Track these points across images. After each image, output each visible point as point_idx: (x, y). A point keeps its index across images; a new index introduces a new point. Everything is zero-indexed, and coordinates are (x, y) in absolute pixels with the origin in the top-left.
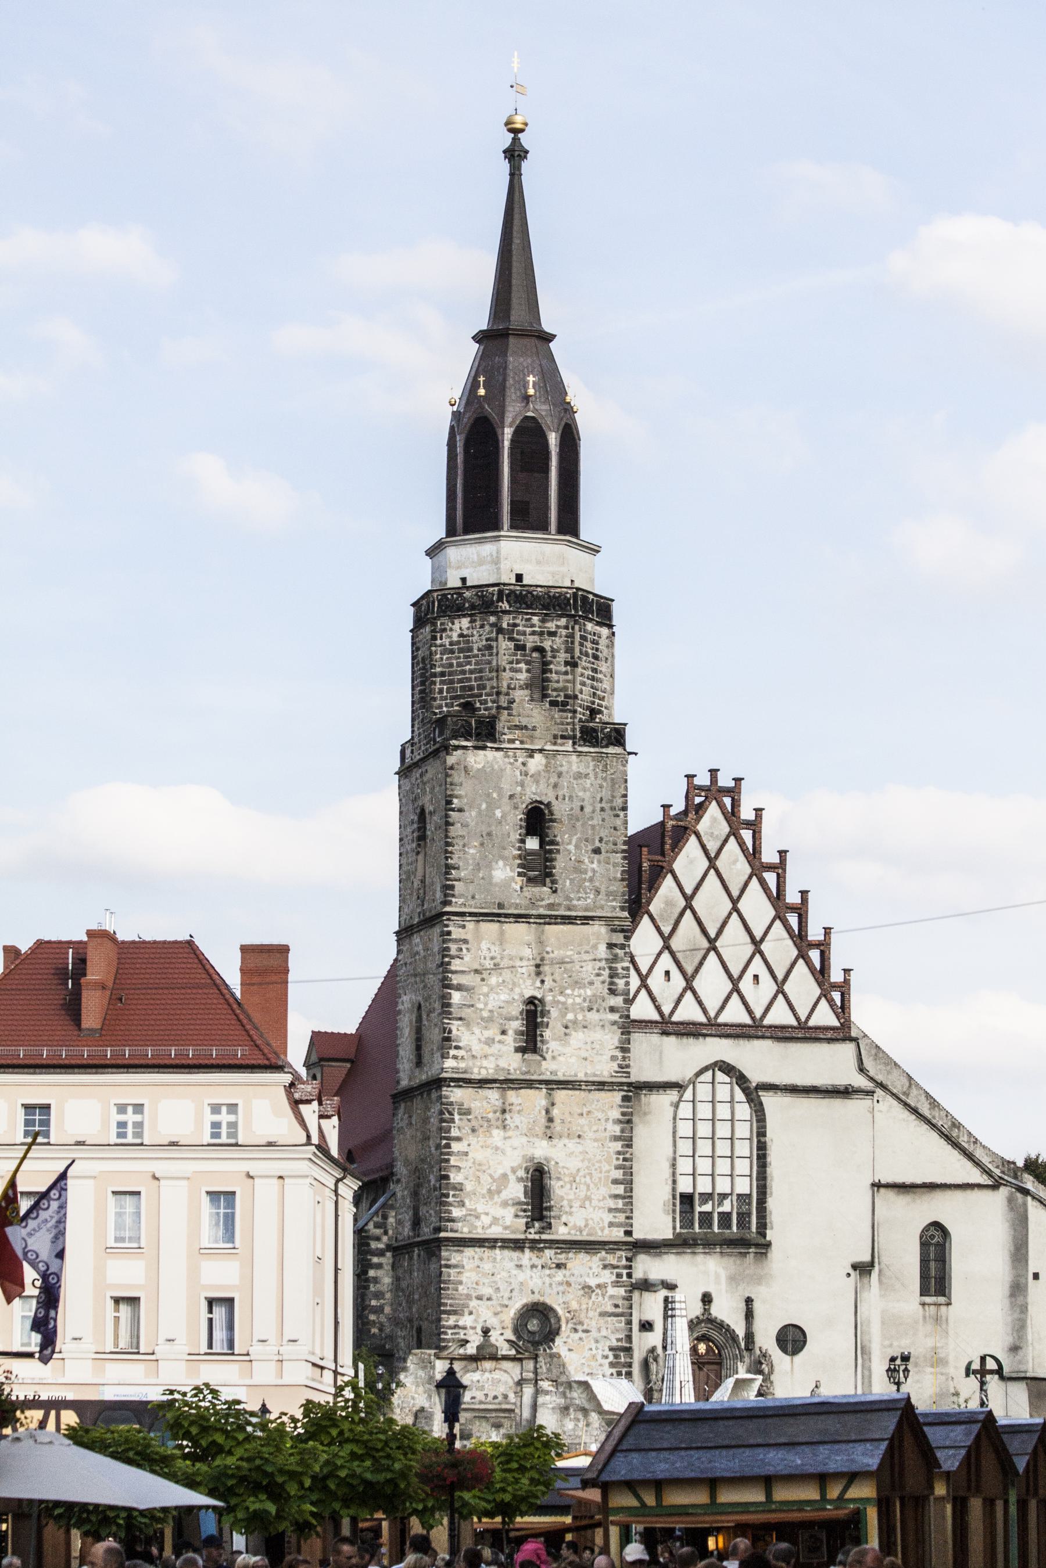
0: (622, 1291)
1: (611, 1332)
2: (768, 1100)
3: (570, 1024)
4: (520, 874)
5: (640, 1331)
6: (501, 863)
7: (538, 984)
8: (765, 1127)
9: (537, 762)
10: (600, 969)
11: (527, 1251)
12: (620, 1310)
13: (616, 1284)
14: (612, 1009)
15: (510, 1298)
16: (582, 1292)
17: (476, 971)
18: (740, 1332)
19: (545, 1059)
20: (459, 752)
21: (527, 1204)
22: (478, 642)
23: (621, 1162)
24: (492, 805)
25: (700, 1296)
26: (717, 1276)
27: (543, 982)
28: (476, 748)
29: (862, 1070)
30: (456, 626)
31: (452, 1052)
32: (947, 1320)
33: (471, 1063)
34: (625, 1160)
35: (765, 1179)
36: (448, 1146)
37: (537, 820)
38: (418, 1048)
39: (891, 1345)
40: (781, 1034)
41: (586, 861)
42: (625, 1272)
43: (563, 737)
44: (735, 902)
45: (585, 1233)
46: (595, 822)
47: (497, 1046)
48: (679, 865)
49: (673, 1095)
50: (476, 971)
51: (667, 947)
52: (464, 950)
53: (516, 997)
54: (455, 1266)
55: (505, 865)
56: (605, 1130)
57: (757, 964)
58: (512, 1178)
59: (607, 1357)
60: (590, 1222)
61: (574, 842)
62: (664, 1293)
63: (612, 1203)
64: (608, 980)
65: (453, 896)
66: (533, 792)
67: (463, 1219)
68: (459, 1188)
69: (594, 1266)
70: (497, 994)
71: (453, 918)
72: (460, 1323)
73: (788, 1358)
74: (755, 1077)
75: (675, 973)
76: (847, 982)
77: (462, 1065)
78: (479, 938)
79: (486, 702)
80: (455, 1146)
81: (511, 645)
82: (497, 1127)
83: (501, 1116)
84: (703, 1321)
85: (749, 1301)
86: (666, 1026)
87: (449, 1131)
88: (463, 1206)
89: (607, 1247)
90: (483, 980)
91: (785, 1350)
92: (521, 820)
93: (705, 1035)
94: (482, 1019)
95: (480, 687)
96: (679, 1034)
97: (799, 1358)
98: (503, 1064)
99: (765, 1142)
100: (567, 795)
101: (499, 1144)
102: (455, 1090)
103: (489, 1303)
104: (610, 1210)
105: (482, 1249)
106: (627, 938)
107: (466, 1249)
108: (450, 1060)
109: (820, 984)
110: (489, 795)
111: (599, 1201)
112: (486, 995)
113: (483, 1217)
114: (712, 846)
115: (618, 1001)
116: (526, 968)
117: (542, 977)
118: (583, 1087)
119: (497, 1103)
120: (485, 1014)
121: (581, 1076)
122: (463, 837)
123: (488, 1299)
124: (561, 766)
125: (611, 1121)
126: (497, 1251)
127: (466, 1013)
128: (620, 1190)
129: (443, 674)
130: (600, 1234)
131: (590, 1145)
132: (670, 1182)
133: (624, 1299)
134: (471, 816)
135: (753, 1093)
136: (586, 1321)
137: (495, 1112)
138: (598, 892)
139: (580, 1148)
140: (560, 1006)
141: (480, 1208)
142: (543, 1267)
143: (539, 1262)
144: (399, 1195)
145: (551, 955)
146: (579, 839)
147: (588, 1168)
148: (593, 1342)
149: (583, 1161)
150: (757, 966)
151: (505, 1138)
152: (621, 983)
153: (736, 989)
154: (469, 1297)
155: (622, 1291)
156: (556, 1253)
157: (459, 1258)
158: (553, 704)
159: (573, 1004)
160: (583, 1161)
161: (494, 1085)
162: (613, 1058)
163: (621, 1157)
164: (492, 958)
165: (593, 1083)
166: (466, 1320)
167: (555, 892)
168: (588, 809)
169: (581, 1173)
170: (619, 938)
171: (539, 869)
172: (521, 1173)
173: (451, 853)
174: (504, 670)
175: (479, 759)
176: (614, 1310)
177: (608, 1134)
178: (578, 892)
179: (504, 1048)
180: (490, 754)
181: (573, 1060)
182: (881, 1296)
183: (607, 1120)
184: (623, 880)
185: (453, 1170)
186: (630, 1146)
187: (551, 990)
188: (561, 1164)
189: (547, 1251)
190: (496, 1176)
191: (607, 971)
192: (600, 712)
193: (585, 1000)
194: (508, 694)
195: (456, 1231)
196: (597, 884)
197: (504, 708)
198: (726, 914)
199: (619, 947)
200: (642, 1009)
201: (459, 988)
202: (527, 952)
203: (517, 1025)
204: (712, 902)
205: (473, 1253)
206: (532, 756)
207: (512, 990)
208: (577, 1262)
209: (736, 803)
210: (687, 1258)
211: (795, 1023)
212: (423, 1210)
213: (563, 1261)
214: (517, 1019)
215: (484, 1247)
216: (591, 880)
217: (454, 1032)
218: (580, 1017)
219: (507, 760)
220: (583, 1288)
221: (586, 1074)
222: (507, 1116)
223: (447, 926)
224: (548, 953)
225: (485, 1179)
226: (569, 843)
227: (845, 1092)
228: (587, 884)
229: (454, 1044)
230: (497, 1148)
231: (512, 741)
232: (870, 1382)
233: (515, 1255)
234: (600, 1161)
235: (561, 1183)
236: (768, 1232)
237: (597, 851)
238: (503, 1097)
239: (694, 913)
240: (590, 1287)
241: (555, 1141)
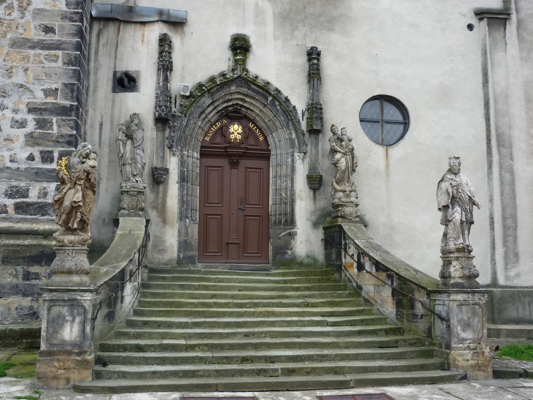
5: (114, 91)
12: (55, 38)
25: (228, 41)
26: (259, 12)
59: (22, 124)
84: (232, 81)
85: (313, 55)
133: (64, 17)
176: (43, 36)
182: (521, 59)
232: (513, 191)
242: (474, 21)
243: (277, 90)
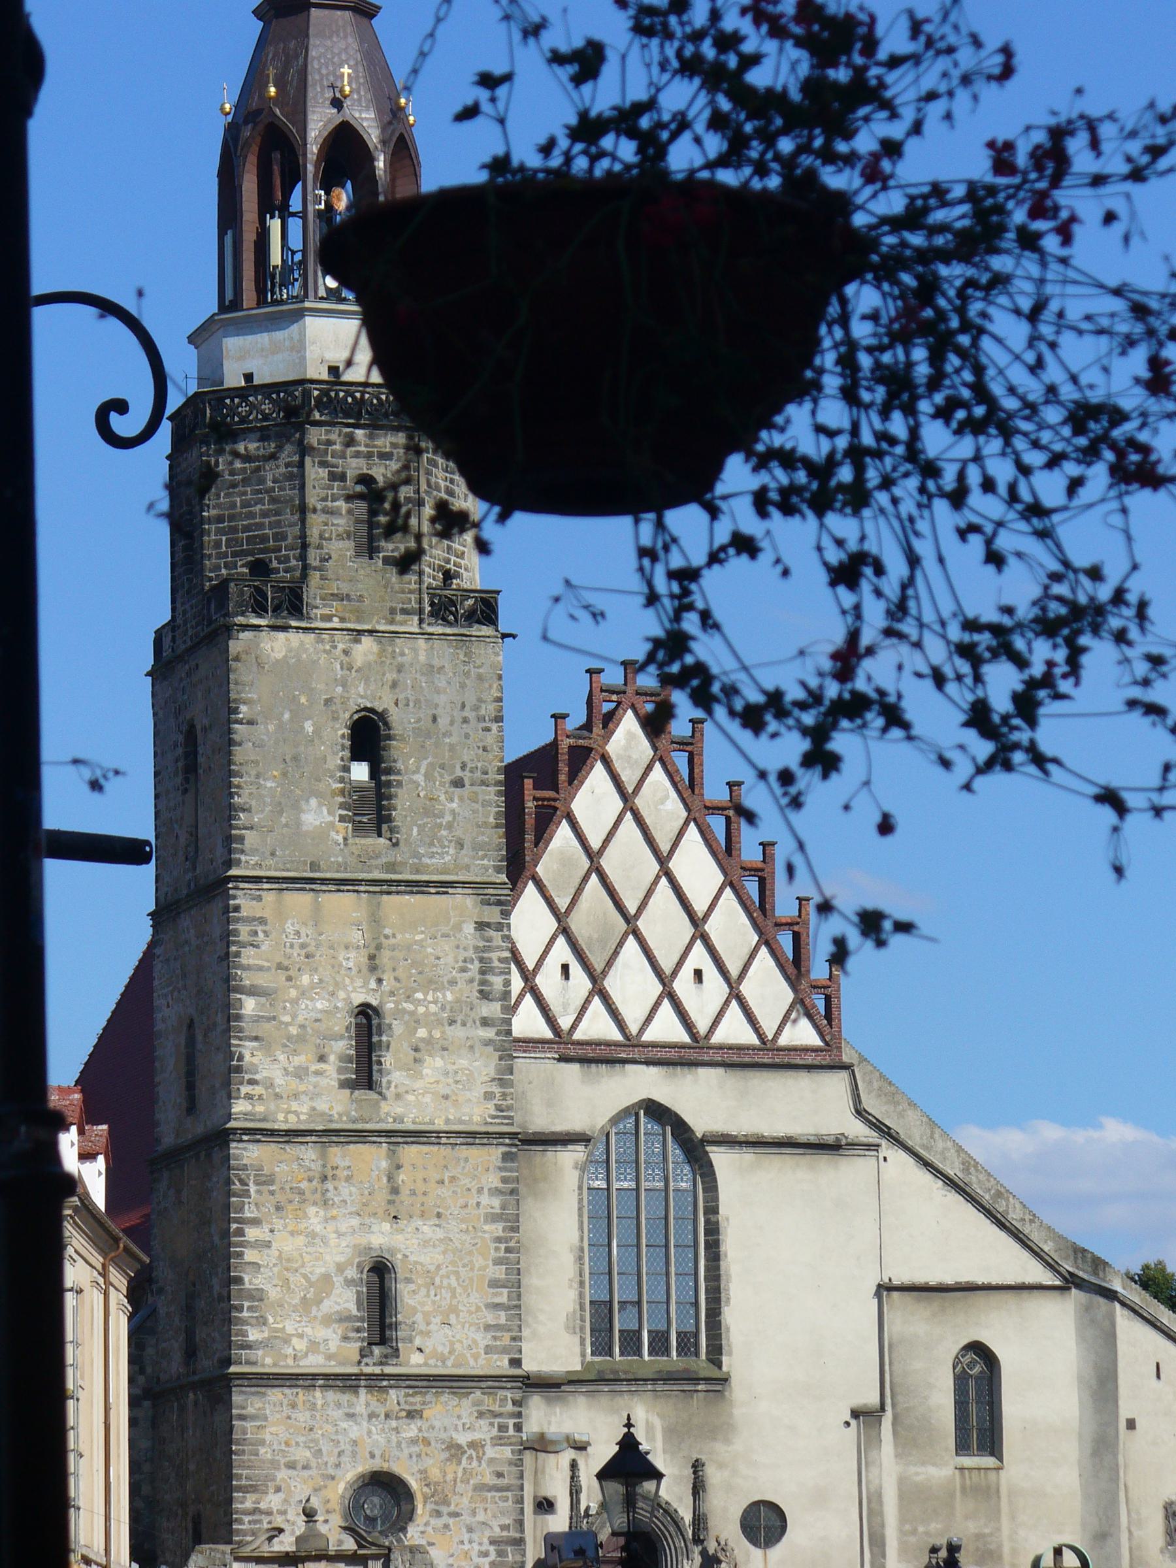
0: (507, 1452)
1: (495, 1517)
2: (720, 1158)
3: (421, 1045)
4: (342, 819)
5: (535, 1513)
6: (313, 802)
7: (373, 984)
8: (716, 1199)
10: (465, 961)
11: (362, 1391)
13: (498, 1441)
14: (485, 1022)
15: (338, 1465)
16: (447, 1455)
17: (280, 967)
18: (686, 1516)
19: (385, 1098)
20: (246, 635)
21: (361, 1320)
23: (502, 1254)
24: (299, 715)
27: (380, 981)
28: (274, 628)
29: (860, 1113)
31: (244, 1090)
32: (998, 1491)
33: (272, 1107)
34: (508, 1250)
35: (717, 1278)
36: (240, 1232)
37: (368, 736)
38: (190, 1087)
39: (914, 1532)
40: (736, 1060)
41: (442, 798)
42: (511, 1422)
43: (405, 612)
44: (663, 861)
45: (449, 1363)
46: (454, 739)
47: (313, 1079)
48: (581, 805)
49: (577, 1153)
50: (280, 967)
52: (261, 935)
53: (339, 1005)
54: (254, 1418)
55: (320, 805)
56: (478, 1204)
58: (338, 1280)
59: (485, 1554)
60: (458, 1346)
61: (423, 771)
62: (569, 1455)
63: (490, 1318)
64: (478, 977)
65: (242, 852)
66: (361, 696)
68: (258, 1296)
69: (465, 1414)
70: (312, 1000)
71: (242, 885)
72: (263, 1506)
73: (757, 1553)
74: (700, 1125)
75: (576, 969)
77: (260, 1109)
79: (287, 559)
80: (252, 1233)
81: (323, 473)
82: (315, 1203)
83: (319, 1186)
85: (697, 1466)
87: (241, 1210)
88: (264, 1324)
89: (483, 1385)
90: (289, 979)
91: (754, 1542)
92: (343, 736)
93: (624, 1062)
94: (289, 1038)
95: (275, 535)
96: (584, 1061)
97: (777, 1552)
98: (322, 1106)
99: (718, 1222)
100: (412, 698)
101: (318, 1229)
102: (250, 1146)
103: (306, 1473)
105: (295, 1390)
106: (506, 914)
107: (269, 1391)
108: (241, 1101)
109: (793, 983)
110: (295, 699)
111: (471, 1313)
112: (295, 1002)
113: (295, 1341)
114: (629, 778)
115: (493, 1009)
116: (354, 959)
117: (379, 974)
118: (444, 1140)
119: (313, 1166)
120: (294, 1030)
121: (440, 1125)
122: (256, 762)
123: (305, 1467)
124: (403, 654)
125: (486, 1190)
126: (318, 1393)
127: (265, 1029)
128: (503, 1297)
129: (220, 519)
130: (472, 1363)
132: (576, 1285)
133: (510, 1463)
134: (267, 730)
135: (695, 1149)
136: (454, 1500)
137: (310, 1180)
138: (460, 845)
139: (440, 1234)
140: (407, 1017)
141: (290, 1329)
142: (387, 1416)
143: (382, 1411)
144: (162, 1311)
145: (392, 941)
146: (431, 764)
147: (453, 1263)
148: (464, 1530)
149: (444, 1253)
150: (699, 957)
151: (326, 1220)
152: (497, 981)
154: (275, 1464)
155: (507, 1452)
156: (407, 1395)
157: (260, 1405)
159: (427, 1014)
160: (444, 1253)
161: (308, 1139)
163: (503, 1246)
164: (303, 946)
165: (458, 1133)
166: (272, 1501)
167: (396, 845)
168: (443, 722)
169: (443, 1272)
170: (492, 914)
171: (373, 810)
172: (352, 1273)
173: (238, 787)
174: (315, 511)
177: (482, 1211)
178: (431, 844)
179: (323, 1082)
180: (294, 638)
181: (427, 1099)
183: (480, 1190)
184: (497, 826)
185: (248, 1269)
186: (516, 1229)
187: (392, 994)
188: (412, 1258)
189: (392, 1392)
190: (313, 1278)
191: (476, 962)
192: (457, 575)
193: (443, 1008)
194: (319, 547)
195: (254, 1363)
196: (458, 833)
197: (315, 569)
198: (652, 878)
199: (494, 925)
200: (528, 1022)
201: (253, 992)
202: (356, 937)
203: (344, 1046)
204: (629, 862)
205: (280, 1396)
206: (358, 641)
207: (333, 994)
208: (439, 1407)
210: (604, 1400)
211: (754, 1040)
212: (201, 1334)
213: (418, 1407)
214: (342, 1037)
215: (297, 1386)
216: (450, 826)
217: (247, 1057)
218: (437, 1034)
219: (320, 646)
220: (448, 1448)
221: (447, 1121)
222: (329, 1185)
223: (234, 897)
224: (387, 937)
225: (296, 1280)
226: (417, 771)
228: (444, 833)
229: (247, 1077)
230: (313, 1235)
231: (328, 618)
233: (345, 1398)
234: (470, 1253)
235: (412, 1287)
236: (724, 1359)
237: (458, 783)
238: (323, 1156)
240: (459, 1447)
241: (402, 1223)
242: (848, 1417)
243: (667, 1503)
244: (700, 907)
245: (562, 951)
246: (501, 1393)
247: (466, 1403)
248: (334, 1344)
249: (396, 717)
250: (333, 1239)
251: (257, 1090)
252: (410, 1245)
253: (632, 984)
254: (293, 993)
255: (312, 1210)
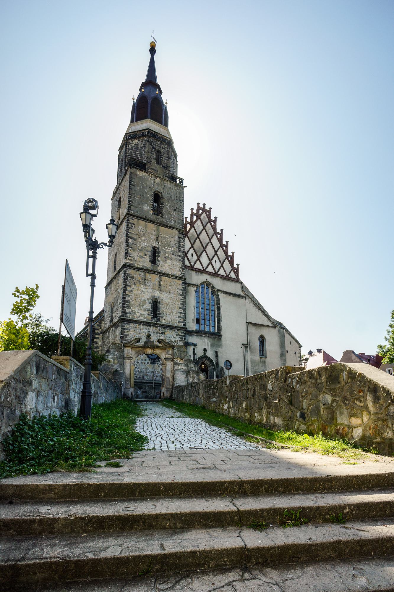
9: (158, 180)
11: (152, 327)
13: (180, 341)
14: (179, 256)
22: (140, 145)
24: (144, 188)
26: (208, 344)
30: (134, 142)
31: (128, 258)
36: (125, 287)
37: (157, 198)
44: (210, 239)
51: (192, 247)
54: (127, 329)
57: (216, 256)
58: (147, 302)
62: (193, 347)
66: (156, 188)
67: (130, 313)
68: (129, 302)
76: (238, 267)
78: (139, 225)
80: (128, 288)
86: (192, 268)
98: (145, 265)
104: (179, 317)
112: (140, 242)
116: (153, 237)
120: (140, 248)
127: (133, 246)
128: (182, 311)
129: (129, 155)
131: (173, 296)
135: (215, 292)
139: (170, 296)
143: (156, 331)
146: (170, 206)
153: (211, 263)
158: (163, 166)
162: (180, 270)
168: (173, 198)
170: (181, 236)
172: (150, 301)
175: (140, 173)
180: (144, 173)
201: (131, 238)
203: (150, 253)
209: (210, 214)
216: (173, 218)
225: (138, 300)
227: (239, 296)
230: (143, 291)
237: (175, 210)
238: (145, 275)
239: (200, 240)
244: (216, 249)
245: (192, 251)
246: (181, 331)
247: (174, 332)
248: (146, 316)
249: (163, 194)
250: (146, 293)
251: (131, 258)
252: (163, 296)
253: (204, 260)
254: (140, 241)
255: (142, 286)
